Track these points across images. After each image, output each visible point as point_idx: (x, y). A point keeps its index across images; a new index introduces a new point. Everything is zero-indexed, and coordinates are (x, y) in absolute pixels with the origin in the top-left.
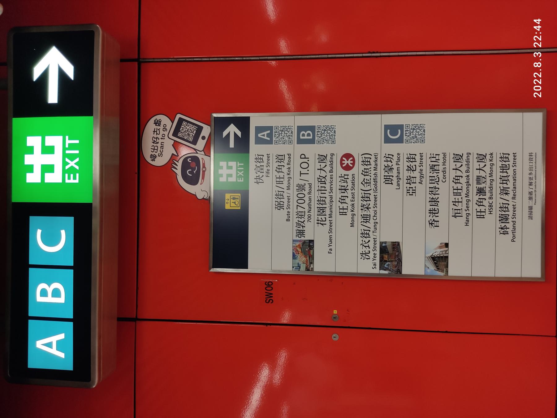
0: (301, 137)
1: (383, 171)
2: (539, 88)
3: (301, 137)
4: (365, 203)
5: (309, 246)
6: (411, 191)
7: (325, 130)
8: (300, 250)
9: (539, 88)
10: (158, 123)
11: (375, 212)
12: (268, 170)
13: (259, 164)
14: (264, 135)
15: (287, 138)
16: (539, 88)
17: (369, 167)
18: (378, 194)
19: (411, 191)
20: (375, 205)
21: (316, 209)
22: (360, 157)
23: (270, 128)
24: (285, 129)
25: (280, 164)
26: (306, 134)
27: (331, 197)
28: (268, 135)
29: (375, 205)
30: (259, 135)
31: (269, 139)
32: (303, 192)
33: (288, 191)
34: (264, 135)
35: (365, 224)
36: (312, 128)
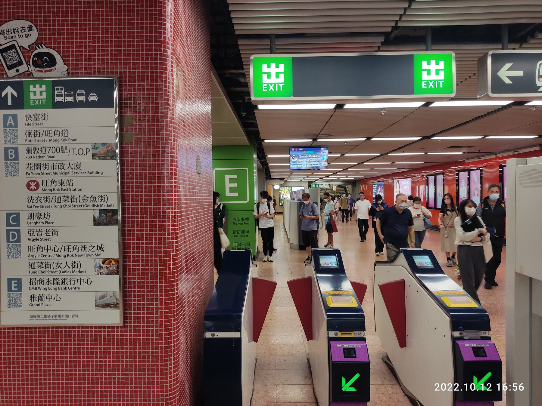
0: (9, 150)
1: (37, 212)
2: (444, 389)
3: (9, 150)
4: (70, 198)
5: (113, 156)
6: (31, 232)
7: (15, 168)
8: (109, 149)
9: (444, 388)
10: (30, 29)
11: (69, 206)
12: (30, 124)
13: (40, 117)
14: (10, 121)
15: (8, 139)
16: (444, 388)
17: (97, 200)
18: (83, 208)
19: (31, 232)
20: (74, 206)
21: (39, 162)
22: (105, 194)
23: (16, 126)
24: (16, 137)
25: (61, 133)
26: (12, 154)
27: (69, 173)
28: (10, 124)
29: (74, 206)
30: (10, 117)
31: (8, 125)
32: (61, 152)
33: (48, 140)
34: (10, 121)
35: (54, 199)
36: (16, 158)
